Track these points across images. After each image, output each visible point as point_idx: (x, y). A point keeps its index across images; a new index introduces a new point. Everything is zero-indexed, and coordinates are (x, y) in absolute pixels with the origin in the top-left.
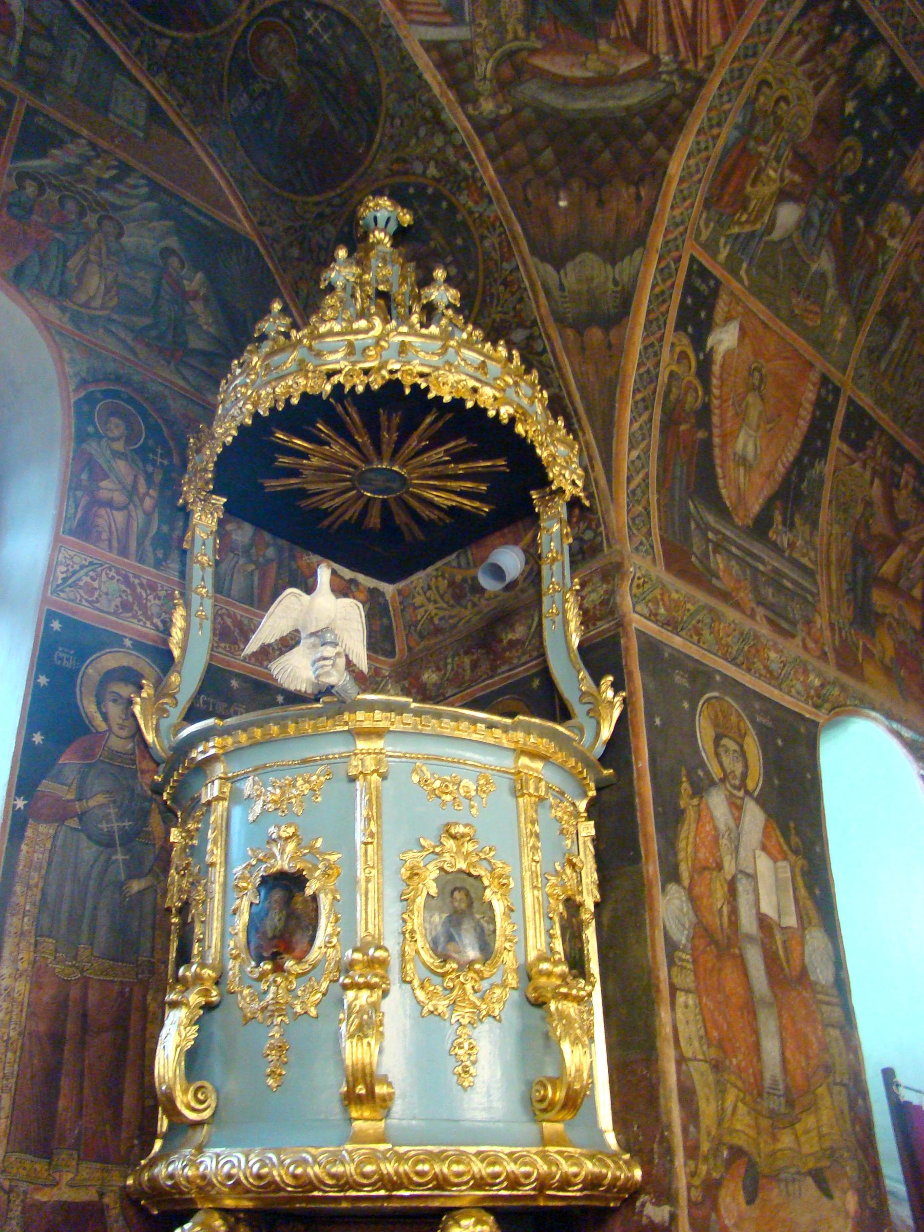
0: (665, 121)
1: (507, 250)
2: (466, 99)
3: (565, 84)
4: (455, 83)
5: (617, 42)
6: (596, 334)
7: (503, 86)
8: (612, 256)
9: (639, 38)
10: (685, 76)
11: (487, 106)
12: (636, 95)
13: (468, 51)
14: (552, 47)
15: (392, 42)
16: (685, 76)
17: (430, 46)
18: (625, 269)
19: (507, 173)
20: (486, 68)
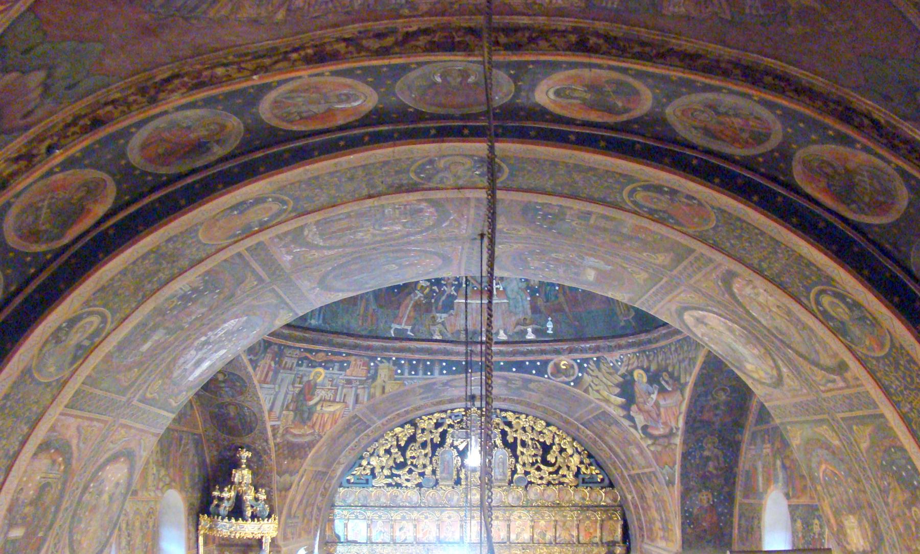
0: (311, 445)
1: (271, 472)
2: (275, 438)
3: (295, 435)
4: (274, 435)
5: (309, 427)
6: (283, 493)
7: (283, 435)
8: (291, 475)
9: (313, 427)
10: (319, 435)
11: (278, 440)
12: (307, 439)
14: (296, 427)
15: (264, 423)
16: (319, 435)
18: (293, 478)
19: (277, 456)
20: (281, 431)
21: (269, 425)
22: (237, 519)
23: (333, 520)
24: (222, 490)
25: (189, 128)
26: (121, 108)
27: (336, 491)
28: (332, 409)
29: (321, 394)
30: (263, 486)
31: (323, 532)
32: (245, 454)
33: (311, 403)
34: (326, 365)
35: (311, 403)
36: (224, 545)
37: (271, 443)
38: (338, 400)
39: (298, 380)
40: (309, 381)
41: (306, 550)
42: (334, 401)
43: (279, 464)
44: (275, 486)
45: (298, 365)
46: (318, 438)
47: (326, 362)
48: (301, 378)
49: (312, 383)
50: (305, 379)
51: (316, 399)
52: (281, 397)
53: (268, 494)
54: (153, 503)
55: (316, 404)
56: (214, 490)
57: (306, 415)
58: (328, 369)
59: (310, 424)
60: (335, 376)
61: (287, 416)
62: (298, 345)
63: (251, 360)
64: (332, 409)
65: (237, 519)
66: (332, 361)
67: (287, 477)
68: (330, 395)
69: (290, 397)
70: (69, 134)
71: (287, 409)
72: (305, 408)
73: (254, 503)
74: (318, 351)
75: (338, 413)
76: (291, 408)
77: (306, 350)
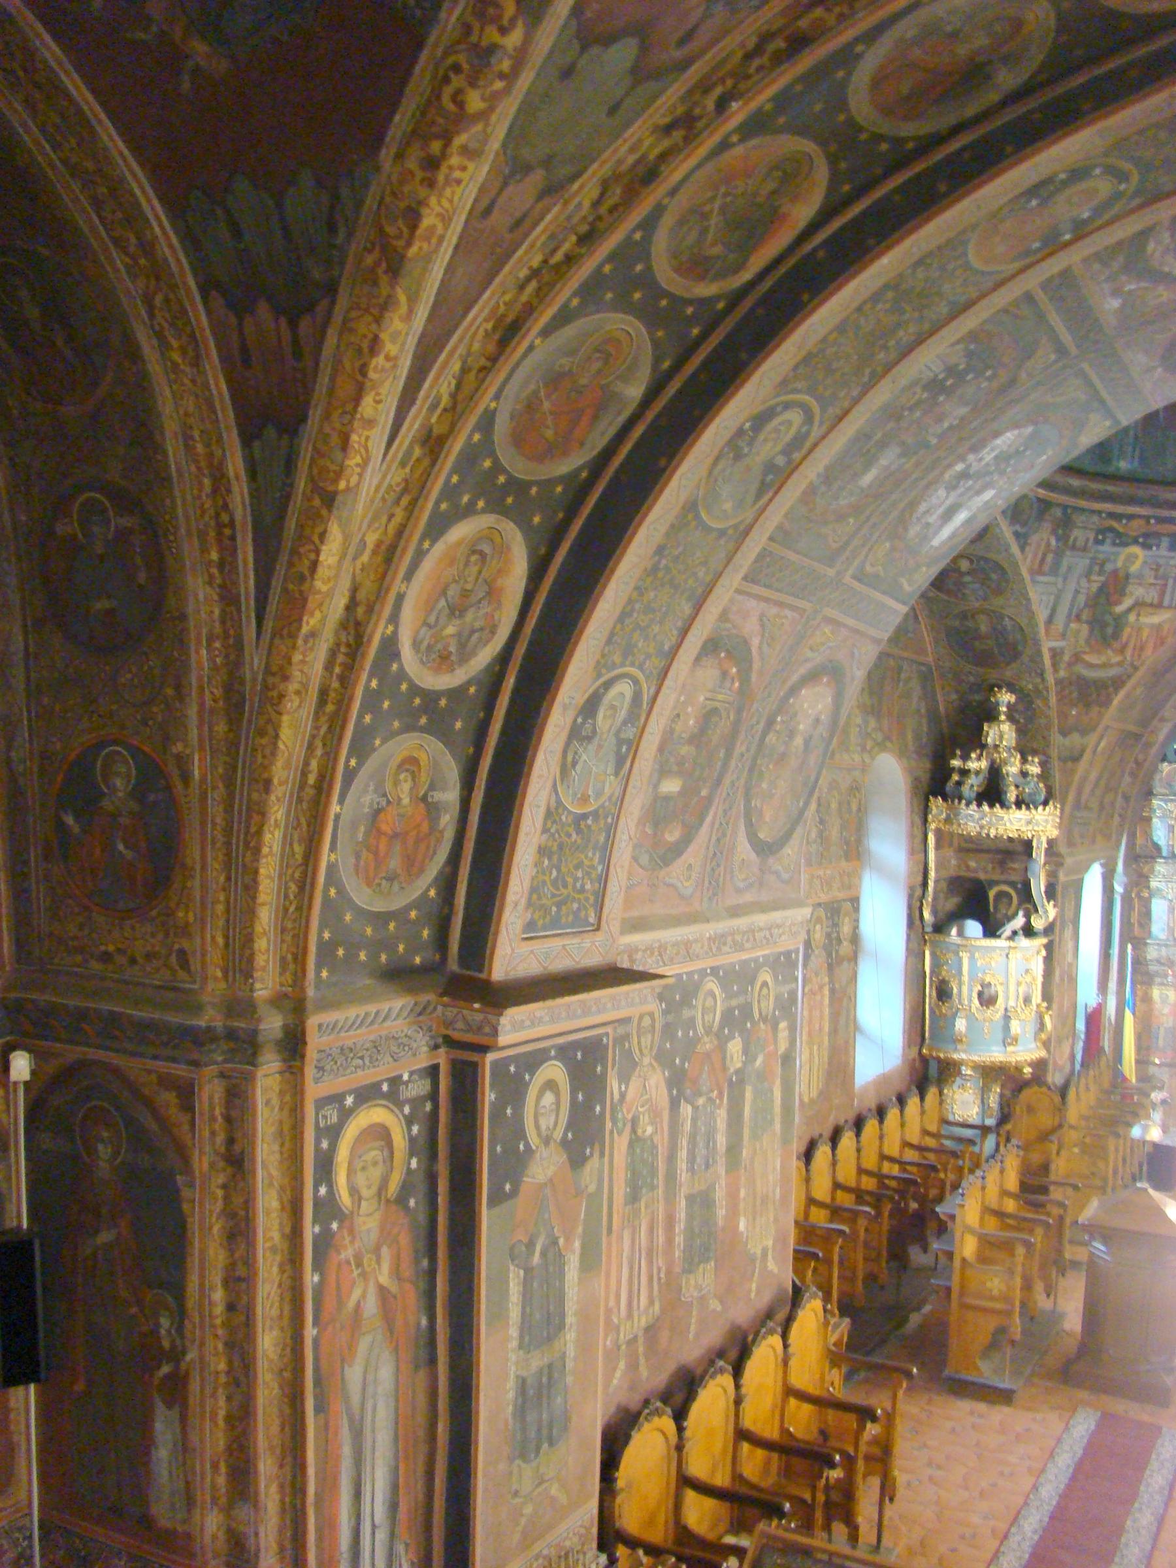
0: (1118, 683)
1: (1048, 727)
3: (1091, 666)
4: (1055, 665)
6: (1070, 764)
7: (1070, 665)
9: (1122, 651)
10: (1132, 665)
11: (1062, 674)
12: (1112, 672)
13: (1062, 652)
15: (1037, 643)
17: (1052, 650)
20: (1066, 658)
21: (1046, 646)
22: (991, 806)
23: (1149, 820)
24: (965, 757)
25: (954, 36)
26: (837, 10)
27: (1155, 770)
28: (1155, 619)
29: (1136, 592)
30: (1035, 753)
31: (1132, 836)
32: (1005, 698)
33: (1119, 609)
34: (1147, 540)
35: (1119, 609)
36: (968, 851)
37: (1050, 679)
38: (1166, 603)
39: (1097, 568)
40: (1115, 572)
41: (1102, 865)
42: (1159, 606)
43: (1063, 715)
44: (1054, 753)
45: (1098, 542)
46: (1130, 670)
47: (1146, 536)
48: (1102, 565)
49: (1121, 574)
50: (1109, 567)
51: (1127, 603)
52: (1068, 597)
53: (1043, 764)
54: (857, 773)
55: (1129, 610)
56: (953, 756)
57: (1110, 631)
58: (1149, 547)
59: (1116, 645)
60: (1161, 561)
61: (1078, 631)
62: (1097, 506)
63: (1017, 535)
64: (1155, 619)
65: (991, 806)
66: (1158, 535)
67: (1075, 739)
68: (1152, 596)
69: (1082, 599)
70: (752, 71)
71: (1078, 618)
72: (1108, 618)
73: (1021, 780)
74: (1131, 517)
75: (1166, 627)
76: (1084, 617)
77: (1112, 515)
